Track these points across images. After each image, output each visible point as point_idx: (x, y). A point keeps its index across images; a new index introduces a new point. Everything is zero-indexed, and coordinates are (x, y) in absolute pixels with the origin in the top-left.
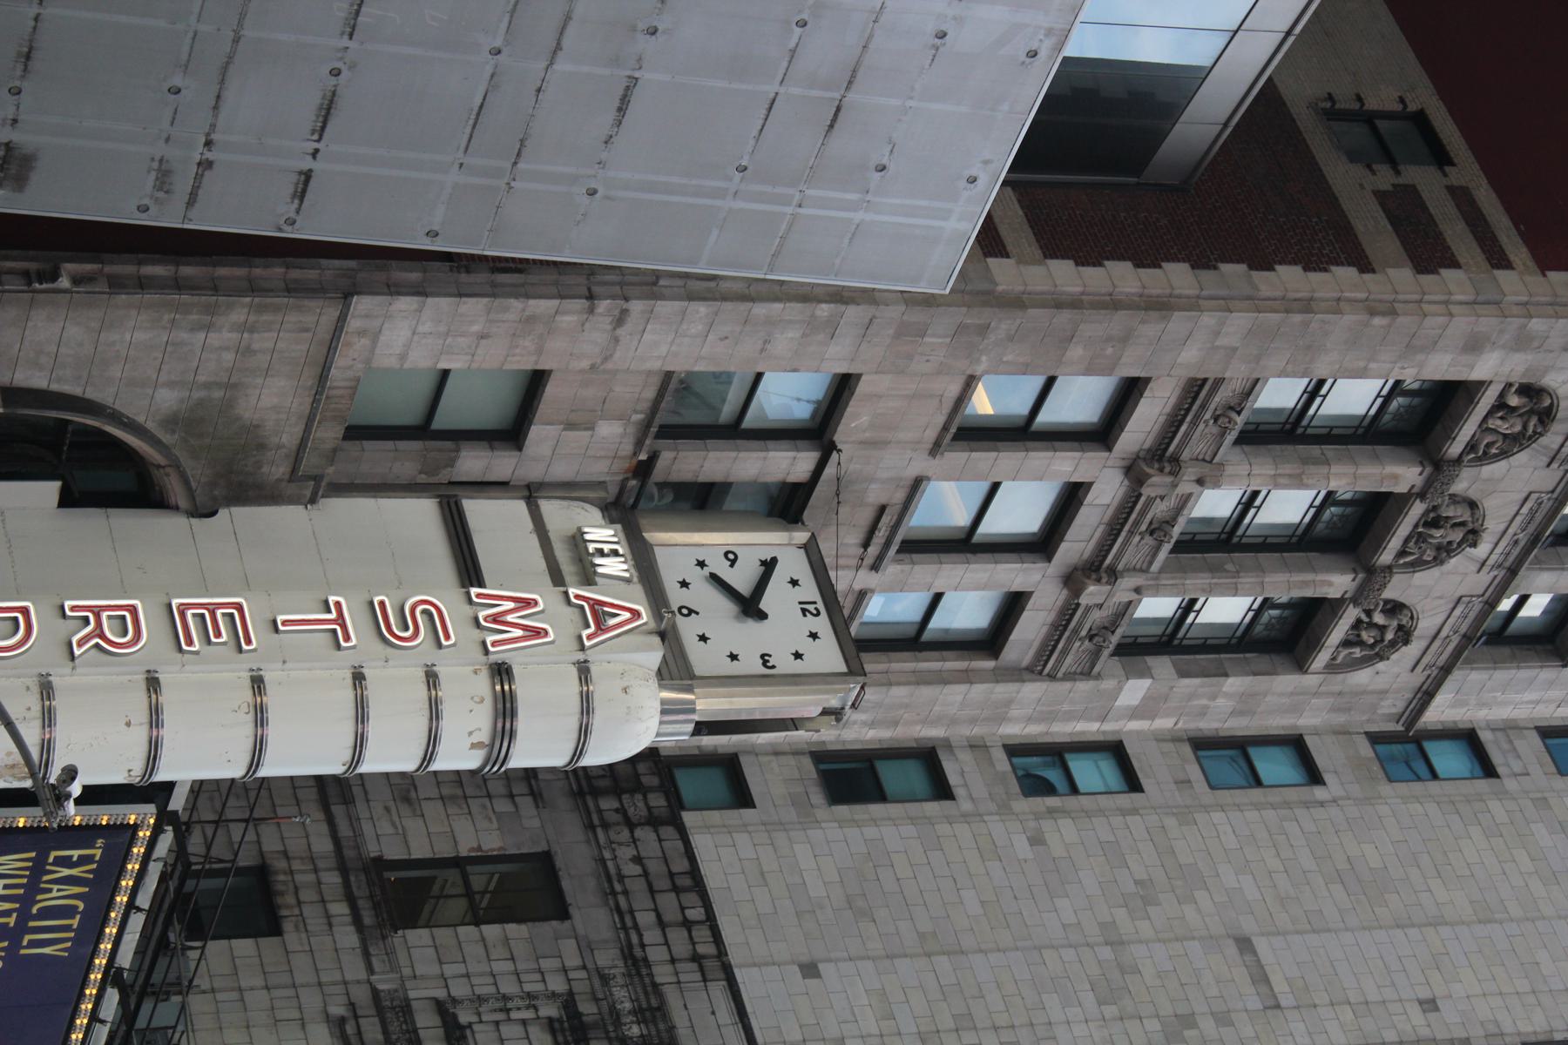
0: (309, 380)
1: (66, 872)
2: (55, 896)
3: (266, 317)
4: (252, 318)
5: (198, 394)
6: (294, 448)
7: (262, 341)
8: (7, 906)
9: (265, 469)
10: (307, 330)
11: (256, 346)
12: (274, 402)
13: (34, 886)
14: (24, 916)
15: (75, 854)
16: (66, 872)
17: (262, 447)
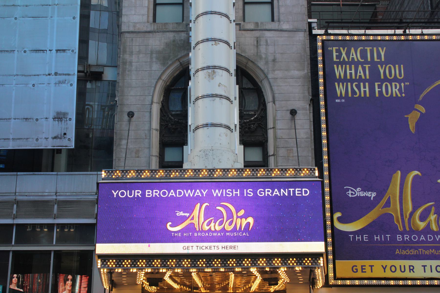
0: (147, 35)
1: (344, 55)
2: (355, 55)
3: (128, 50)
4: (128, 53)
5: (154, 60)
6: (175, 33)
7: (136, 49)
8: (360, 68)
9: (182, 38)
10: (132, 40)
11: (138, 50)
12: (157, 42)
13: (352, 62)
14: (366, 62)
15: (335, 54)
16: (344, 55)
17: (174, 41)
